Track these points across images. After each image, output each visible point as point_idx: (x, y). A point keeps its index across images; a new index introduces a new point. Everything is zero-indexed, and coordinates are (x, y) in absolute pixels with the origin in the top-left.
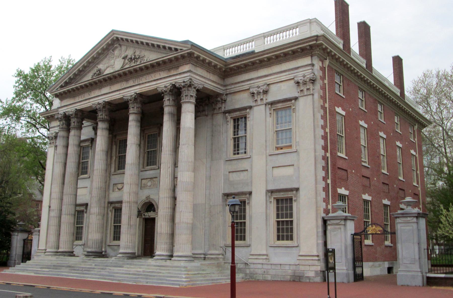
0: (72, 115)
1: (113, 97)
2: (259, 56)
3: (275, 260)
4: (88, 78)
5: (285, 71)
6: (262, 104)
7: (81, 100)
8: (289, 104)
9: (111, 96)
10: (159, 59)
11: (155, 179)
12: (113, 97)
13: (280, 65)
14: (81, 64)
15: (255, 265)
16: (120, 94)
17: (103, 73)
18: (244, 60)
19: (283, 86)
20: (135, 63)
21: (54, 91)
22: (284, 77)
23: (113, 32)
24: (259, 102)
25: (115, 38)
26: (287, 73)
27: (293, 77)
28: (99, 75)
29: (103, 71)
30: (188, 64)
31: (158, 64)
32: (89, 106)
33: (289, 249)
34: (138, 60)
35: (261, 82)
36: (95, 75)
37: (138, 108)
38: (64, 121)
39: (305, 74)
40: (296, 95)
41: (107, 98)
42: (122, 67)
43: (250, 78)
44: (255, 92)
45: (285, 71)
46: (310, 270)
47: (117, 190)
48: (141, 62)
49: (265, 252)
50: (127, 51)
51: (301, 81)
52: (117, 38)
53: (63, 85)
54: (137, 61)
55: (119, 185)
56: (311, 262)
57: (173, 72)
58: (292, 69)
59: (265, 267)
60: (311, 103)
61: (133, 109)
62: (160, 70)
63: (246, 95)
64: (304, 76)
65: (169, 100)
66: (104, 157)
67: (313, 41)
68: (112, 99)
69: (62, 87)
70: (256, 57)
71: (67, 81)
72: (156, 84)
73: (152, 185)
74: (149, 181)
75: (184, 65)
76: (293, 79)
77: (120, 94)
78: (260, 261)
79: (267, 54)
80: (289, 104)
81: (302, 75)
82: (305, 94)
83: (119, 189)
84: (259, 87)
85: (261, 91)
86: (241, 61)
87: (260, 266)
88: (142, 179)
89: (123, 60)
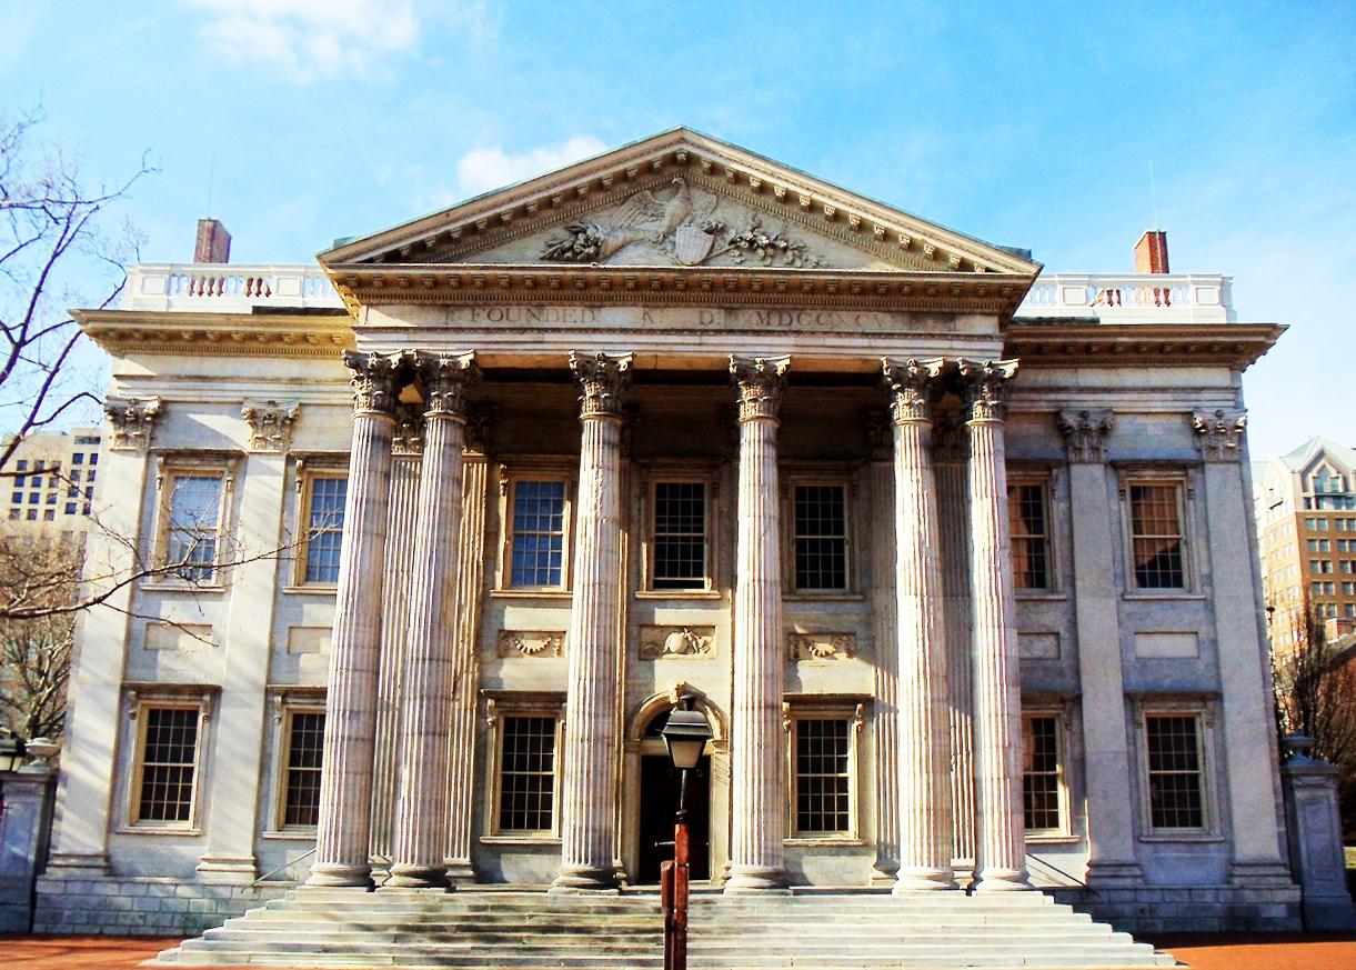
2: (1106, 335)
3: (1160, 876)
4: (525, 256)
5: (1163, 390)
7: (486, 323)
9: (657, 344)
14: (511, 200)
16: (700, 344)
17: (607, 258)
19: (1153, 427)
20: (764, 258)
21: (351, 262)
22: (1157, 403)
23: (680, 135)
24: (1086, 455)
25: (681, 157)
26: (1168, 396)
28: (589, 259)
29: (610, 249)
33: (1197, 848)
35: (1090, 401)
36: (569, 254)
39: (1225, 410)
40: (1192, 455)
42: (703, 262)
45: (1163, 390)
49: (1129, 856)
50: (719, 211)
52: (691, 160)
54: (772, 257)
57: (930, 326)
60: (1239, 484)
63: (1037, 429)
65: (910, 405)
67: (1261, 334)
69: (393, 257)
70: (1098, 335)
71: (430, 244)
72: (870, 347)
75: (975, 313)
77: (700, 344)
78: (1128, 882)
79: (1130, 335)
82: (1222, 458)
84: (1084, 415)
85: (1093, 426)
89: (712, 237)
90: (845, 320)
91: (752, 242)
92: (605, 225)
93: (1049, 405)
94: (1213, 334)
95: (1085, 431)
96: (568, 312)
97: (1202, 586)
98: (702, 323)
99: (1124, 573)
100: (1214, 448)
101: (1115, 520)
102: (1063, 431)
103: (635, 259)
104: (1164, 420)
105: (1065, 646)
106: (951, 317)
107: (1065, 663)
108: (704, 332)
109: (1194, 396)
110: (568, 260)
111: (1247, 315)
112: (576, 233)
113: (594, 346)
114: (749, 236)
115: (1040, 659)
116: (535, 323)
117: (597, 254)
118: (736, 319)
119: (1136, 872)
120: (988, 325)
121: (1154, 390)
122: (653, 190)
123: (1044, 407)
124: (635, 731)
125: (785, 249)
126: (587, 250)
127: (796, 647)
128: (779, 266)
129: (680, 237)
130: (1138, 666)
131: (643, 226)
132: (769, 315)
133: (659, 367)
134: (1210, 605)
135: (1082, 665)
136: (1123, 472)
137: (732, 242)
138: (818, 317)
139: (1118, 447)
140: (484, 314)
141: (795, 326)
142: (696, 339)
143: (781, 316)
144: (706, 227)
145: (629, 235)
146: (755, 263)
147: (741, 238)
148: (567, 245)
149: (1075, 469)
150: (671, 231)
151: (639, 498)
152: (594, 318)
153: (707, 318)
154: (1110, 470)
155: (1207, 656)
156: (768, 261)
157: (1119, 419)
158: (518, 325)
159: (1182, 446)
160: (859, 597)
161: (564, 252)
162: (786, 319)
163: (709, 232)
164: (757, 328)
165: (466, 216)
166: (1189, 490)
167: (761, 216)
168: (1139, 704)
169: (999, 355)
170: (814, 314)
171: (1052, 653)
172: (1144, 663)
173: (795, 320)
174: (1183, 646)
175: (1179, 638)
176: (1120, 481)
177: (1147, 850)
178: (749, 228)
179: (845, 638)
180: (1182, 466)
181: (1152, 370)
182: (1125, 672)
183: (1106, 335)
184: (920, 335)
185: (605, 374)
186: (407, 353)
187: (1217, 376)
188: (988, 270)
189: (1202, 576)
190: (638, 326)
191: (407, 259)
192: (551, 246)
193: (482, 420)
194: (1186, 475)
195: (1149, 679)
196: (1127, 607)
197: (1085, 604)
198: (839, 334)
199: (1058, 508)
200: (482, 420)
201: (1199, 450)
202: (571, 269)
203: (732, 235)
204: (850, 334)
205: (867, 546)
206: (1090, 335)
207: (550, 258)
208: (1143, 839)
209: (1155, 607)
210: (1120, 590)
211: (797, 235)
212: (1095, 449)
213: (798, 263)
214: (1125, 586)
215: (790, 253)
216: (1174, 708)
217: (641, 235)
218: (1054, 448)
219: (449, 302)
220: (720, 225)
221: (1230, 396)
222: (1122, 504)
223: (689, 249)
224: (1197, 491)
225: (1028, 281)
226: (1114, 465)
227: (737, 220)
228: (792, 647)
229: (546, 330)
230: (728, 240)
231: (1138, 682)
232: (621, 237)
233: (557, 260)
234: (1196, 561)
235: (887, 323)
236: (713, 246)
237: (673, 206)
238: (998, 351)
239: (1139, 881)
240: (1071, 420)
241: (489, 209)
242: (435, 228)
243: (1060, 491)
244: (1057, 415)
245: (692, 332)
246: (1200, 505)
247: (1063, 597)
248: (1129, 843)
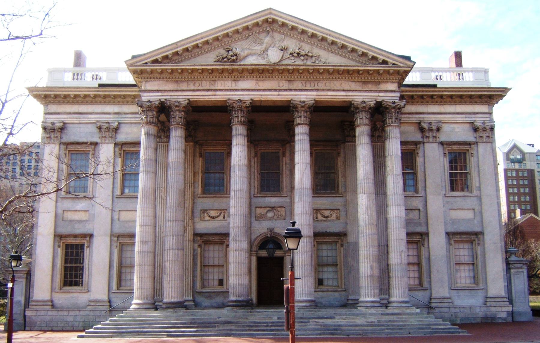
0: (176, 106)
1: (263, 97)
2: (439, 91)
3: (458, 302)
6: (435, 143)
7: (192, 88)
8: (466, 148)
9: (261, 95)
10: (350, 66)
11: (279, 209)
12: (263, 97)
13: (454, 106)
14: (202, 38)
15: (440, 308)
17: (241, 60)
18: (419, 91)
19: (458, 129)
20: (303, 60)
22: (459, 119)
24: (431, 139)
27: (472, 122)
28: (234, 61)
29: (242, 57)
30: (394, 82)
31: (348, 71)
32: (210, 100)
33: (473, 292)
34: (309, 59)
35: (433, 118)
36: (225, 60)
37: (306, 117)
38: (155, 113)
39: (486, 122)
41: (258, 96)
42: (279, 62)
43: (418, 111)
44: (427, 128)
45: (462, 113)
46: (503, 311)
47: (208, 218)
48: (315, 62)
49: (447, 295)
51: (480, 128)
53: (160, 60)
54: (307, 59)
55: (212, 212)
56: (502, 303)
57: (370, 87)
58: (470, 113)
59: (453, 310)
60: (491, 151)
61: (305, 119)
62: (349, 80)
64: (484, 123)
66: (245, 173)
68: (262, 99)
69: (156, 62)
72: (346, 96)
73: (275, 217)
74: (270, 210)
75: (388, 82)
76: (472, 123)
77: (278, 95)
78: (446, 305)
79: (449, 91)
80: (466, 148)
81: (482, 122)
82: (485, 141)
83: (213, 218)
84: (430, 123)
85: (434, 128)
86: (416, 92)
87: (446, 310)
88: (256, 207)
89: (283, 52)
90: (337, 84)
91: (298, 54)
93: (415, 119)
94: (482, 91)
95: (431, 130)
96: (225, 83)
97: (476, 191)
98: (279, 87)
99: (445, 186)
100: (481, 137)
101: (442, 165)
102: (422, 130)
103: (252, 60)
104: (462, 125)
105: (422, 214)
106: (379, 83)
107: (422, 221)
108: (280, 90)
109: (473, 116)
110: (225, 62)
111: (494, 84)
112: (228, 51)
113: (235, 96)
114: (297, 51)
115: (412, 219)
116: (213, 88)
117: (237, 59)
118: (293, 84)
119: (450, 300)
120: (393, 86)
121: (458, 113)
122: (259, 33)
123: (414, 120)
124: (254, 249)
125: (312, 57)
126: (233, 58)
127: (317, 215)
128: (309, 63)
129: (270, 52)
130: (451, 222)
131: (255, 48)
132: (306, 83)
133: (262, 105)
134: (480, 198)
135: (429, 221)
136: (445, 146)
137: (291, 54)
138: (325, 84)
139: (443, 138)
140: (192, 84)
141: (316, 87)
142: (276, 93)
143: (310, 83)
144: (280, 48)
145: (249, 51)
146: (299, 62)
147: (294, 52)
148: (225, 56)
149: (426, 145)
150: (266, 50)
151: (254, 158)
152: (236, 85)
153: (281, 84)
154: (440, 145)
155: (478, 218)
156: (305, 61)
157: (444, 125)
158: (206, 88)
159: (469, 137)
160: (341, 195)
161: (223, 58)
162: (312, 84)
163: (282, 50)
164: (301, 88)
165: (184, 45)
166: (472, 153)
167: (302, 44)
168: (451, 236)
169: (398, 98)
170: (324, 82)
171: (417, 217)
172: (454, 221)
173: (316, 85)
174: (469, 215)
175: (467, 211)
176: (444, 149)
177: (454, 293)
178: (297, 48)
179: (335, 211)
180: (469, 144)
181: (457, 106)
182: (446, 224)
183: (439, 91)
184: (366, 91)
185: (241, 107)
186: (162, 100)
187: (483, 108)
188: (393, 64)
189: (476, 187)
190: (254, 88)
191: (161, 63)
192: (218, 56)
193: (191, 127)
194: (470, 147)
195: (455, 227)
196: (446, 199)
197: (430, 198)
198: (334, 90)
199: (419, 161)
200: (191, 127)
201: (476, 138)
202: (227, 66)
203: (291, 51)
204: (338, 90)
205: (344, 176)
206: (433, 91)
207: (218, 61)
208: (452, 288)
209: (458, 199)
210: (444, 192)
211: (316, 51)
212: (435, 137)
213: (317, 62)
214: (446, 191)
215: (314, 58)
216: (465, 238)
217: (254, 52)
218: (417, 137)
219: (178, 80)
220: (286, 47)
221: (488, 116)
222: (445, 159)
223: (274, 56)
224: (474, 153)
225: (410, 69)
226: (442, 143)
227: (292, 45)
228: (315, 215)
229: (217, 90)
230: (289, 53)
231: (451, 229)
232: (246, 52)
233: (221, 62)
234: (474, 181)
235: (353, 86)
236: (283, 56)
237: (267, 40)
238: (397, 97)
239: (451, 304)
240: (425, 126)
241: (193, 41)
242: (172, 50)
243: (421, 154)
244: (419, 123)
245: (275, 90)
246: (476, 159)
247: (421, 195)
248: (447, 289)
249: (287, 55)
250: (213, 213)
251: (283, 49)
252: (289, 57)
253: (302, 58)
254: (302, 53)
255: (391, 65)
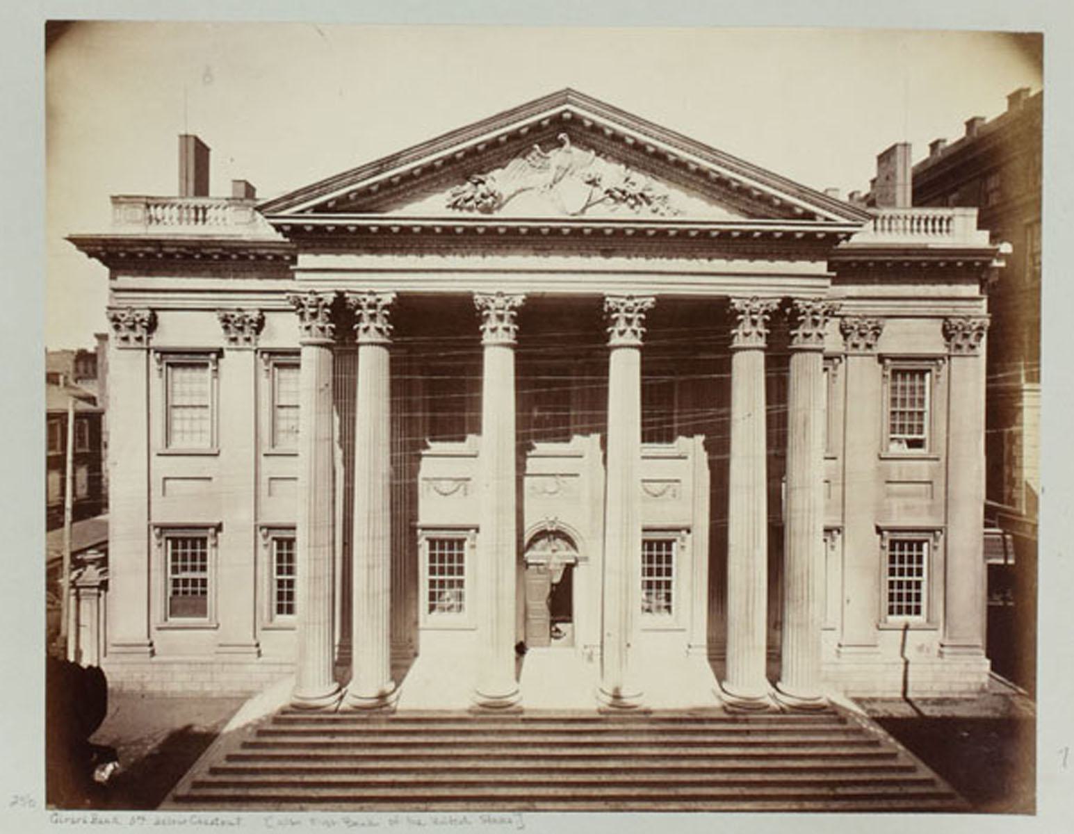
92: (500, 180)
110: (470, 209)
114: (623, 187)
126: (485, 201)
137: (608, 191)
146: (623, 212)
148: (468, 195)
161: (467, 201)
163: (589, 183)
188: (827, 219)
227: (612, 173)
233: (461, 208)
236: (590, 197)
249: (599, 193)
250: (446, 486)
251: (593, 182)
252: (602, 201)
253: (632, 202)
254: (632, 190)
255: (820, 220)
